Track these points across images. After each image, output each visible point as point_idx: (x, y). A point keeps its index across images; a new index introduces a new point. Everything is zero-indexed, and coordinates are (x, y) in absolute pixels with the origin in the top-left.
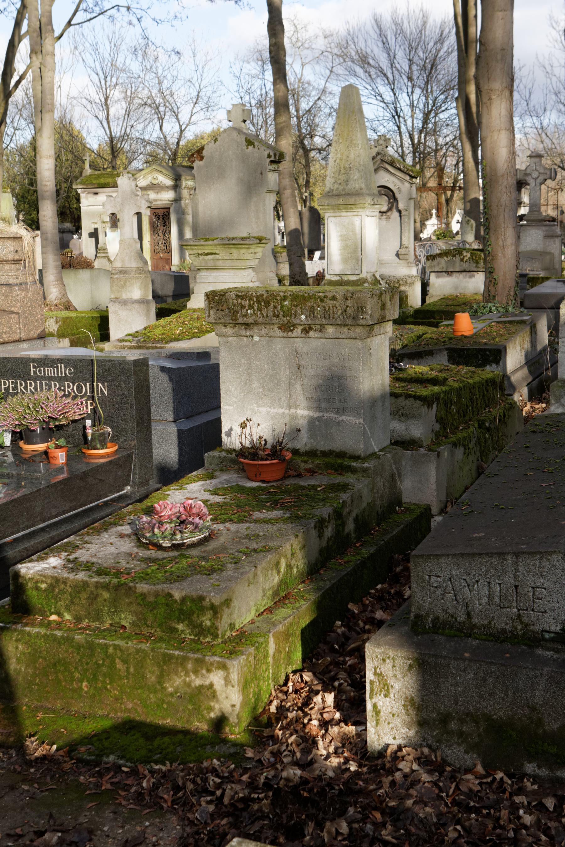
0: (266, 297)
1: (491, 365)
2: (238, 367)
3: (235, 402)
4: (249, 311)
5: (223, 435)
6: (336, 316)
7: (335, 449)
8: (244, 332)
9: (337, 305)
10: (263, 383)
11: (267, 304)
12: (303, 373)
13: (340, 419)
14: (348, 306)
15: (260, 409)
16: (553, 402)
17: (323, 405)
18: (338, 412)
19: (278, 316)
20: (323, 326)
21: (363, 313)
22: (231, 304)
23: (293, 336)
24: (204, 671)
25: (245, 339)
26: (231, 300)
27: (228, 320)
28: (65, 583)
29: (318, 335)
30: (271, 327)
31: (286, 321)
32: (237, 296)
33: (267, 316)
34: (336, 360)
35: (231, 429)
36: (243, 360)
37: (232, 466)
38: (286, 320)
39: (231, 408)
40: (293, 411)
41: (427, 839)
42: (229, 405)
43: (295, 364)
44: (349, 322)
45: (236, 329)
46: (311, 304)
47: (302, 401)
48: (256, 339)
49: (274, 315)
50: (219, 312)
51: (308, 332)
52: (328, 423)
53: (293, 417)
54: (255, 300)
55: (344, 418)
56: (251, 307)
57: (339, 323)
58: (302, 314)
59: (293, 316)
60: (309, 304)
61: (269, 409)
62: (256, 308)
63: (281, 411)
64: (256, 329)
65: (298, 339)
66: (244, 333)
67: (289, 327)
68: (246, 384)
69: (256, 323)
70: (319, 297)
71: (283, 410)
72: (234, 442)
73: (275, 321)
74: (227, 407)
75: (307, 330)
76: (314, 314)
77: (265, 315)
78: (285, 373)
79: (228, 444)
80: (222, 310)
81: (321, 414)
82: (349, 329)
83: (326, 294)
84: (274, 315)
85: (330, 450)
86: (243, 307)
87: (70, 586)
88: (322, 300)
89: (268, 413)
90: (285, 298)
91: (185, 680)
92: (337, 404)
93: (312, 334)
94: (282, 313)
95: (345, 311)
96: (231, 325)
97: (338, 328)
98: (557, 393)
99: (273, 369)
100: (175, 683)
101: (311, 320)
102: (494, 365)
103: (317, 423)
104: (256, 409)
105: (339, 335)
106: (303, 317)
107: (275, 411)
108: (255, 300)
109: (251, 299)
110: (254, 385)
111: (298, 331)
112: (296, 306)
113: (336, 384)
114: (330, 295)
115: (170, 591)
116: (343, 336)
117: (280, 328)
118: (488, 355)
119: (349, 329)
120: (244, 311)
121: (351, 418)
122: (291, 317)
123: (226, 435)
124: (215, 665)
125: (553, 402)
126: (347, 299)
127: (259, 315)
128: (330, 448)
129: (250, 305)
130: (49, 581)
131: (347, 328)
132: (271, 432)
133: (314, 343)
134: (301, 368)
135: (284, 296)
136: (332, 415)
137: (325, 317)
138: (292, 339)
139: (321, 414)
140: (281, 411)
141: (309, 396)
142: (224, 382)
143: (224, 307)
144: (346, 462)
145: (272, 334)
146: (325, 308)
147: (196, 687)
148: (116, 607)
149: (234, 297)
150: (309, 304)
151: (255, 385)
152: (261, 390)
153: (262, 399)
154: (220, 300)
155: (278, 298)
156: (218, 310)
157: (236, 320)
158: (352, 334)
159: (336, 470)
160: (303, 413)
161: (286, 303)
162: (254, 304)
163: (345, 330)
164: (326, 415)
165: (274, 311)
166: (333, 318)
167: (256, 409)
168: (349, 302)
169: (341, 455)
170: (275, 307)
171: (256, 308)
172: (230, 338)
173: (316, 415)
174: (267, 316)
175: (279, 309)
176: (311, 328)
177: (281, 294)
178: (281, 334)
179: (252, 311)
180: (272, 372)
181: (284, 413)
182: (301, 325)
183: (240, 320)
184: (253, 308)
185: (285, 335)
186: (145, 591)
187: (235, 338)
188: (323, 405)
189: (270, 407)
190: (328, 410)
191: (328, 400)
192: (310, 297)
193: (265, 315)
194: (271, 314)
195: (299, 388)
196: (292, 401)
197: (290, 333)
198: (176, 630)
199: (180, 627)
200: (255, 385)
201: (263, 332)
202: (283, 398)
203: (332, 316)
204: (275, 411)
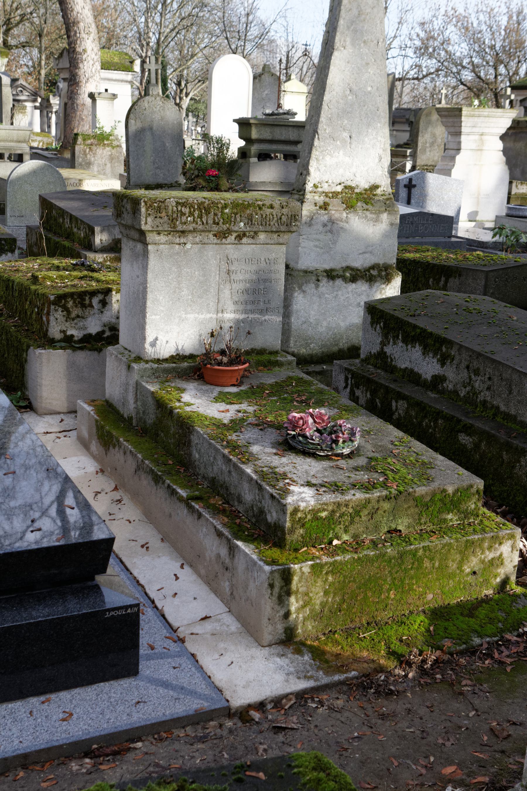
0: (208, 205)
1: (7, 254)
2: (168, 275)
3: (163, 311)
4: (189, 219)
5: (147, 346)
6: (272, 223)
7: (257, 347)
8: (178, 239)
9: (274, 213)
10: (193, 290)
11: (208, 212)
12: (232, 278)
13: (263, 319)
14: (283, 214)
15: (188, 316)
16: (297, 289)
17: (249, 307)
18: (262, 312)
19: (218, 224)
20: (256, 233)
21: (296, 220)
22: (170, 211)
23: (226, 242)
24: (497, 546)
25: (177, 246)
26: (170, 207)
27: (166, 227)
28: (347, 506)
29: (250, 241)
30: (207, 234)
31: (225, 228)
32: (178, 203)
33: (207, 223)
34: (263, 265)
35: (156, 339)
36: (174, 268)
37: (165, 376)
38: (225, 227)
39: (158, 317)
40: (220, 315)
41: (503, 634)
42: (156, 315)
43: (225, 270)
44: (283, 228)
45: (170, 236)
46: (251, 212)
47: (230, 306)
48: (188, 246)
49: (214, 223)
50: (158, 220)
51: (241, 239)
52: (252, 323)
53: (220, 321)
54: (196, 207)
55: (267, 317)
56: (191, 214)
57: (274, 230)
58: (241, 221)
59: (233, 224)
60: (248, 212)
61: (196, 315)
62: (196, 215)
63: (209, 316)
64: (190, 237)
65: (230, 246)
66: (177, 240)
67: (225, 234)
68: (175, 292)
69: (195, 230)
70: (258, 205)
71: (211, 315)
72: (158, 351)
73: (215, 228)
74: (154, 317)
75: (240, 237)
76: (251, 221)
77: (205, 222)
78: (215, 278)
79: (152, 355)
80: (160, 217)
81: (247, 316)
82: (279, 236)
83: (265, 202)
84: (214, 223)
85: (252, 349)
86: (185, 214)
87: (352, 507)
88: (260, 208)
89: (196, 319)
90: (225, 206)
91: (481, 558)
92: (262, 305)
93: (244, 240)
94: (222, 220)
95: (281, 218)
96: (166, 233)
97: (270, 234)
98: (300, 282)
99: (204, 275)
100: (474, 562)
101: (250, 227)
102: (9, 254)
103: (242, 324)
104: (184, 316)
105: (269, 241)
106: (242, 224)
107: (202, 317)
108: (196, 207)
109: (191, 206)
110: (183, 293)
111: (232, 238)
112: (236, 214)
113: (262, 287)
114: (268, 203)
115: (445, 487)
116: (272, 242)
117: (215, 235)
118: (4, 245)
119: (279, 236)
120: (184, 219)
121: (273, 317)
122: (230, 224)
123: (151, 345)
124: (506, 537)
125: (297, 289)
126: (283, 208)
127: (199, 223)
128: (252, 346)
129: (190, 212)
130: (330, 508)
131: (277, 234)
132: (198, 337)
133: (247, 248)
134: (231, 274)
135: (225, 204)
136: (257, 316)
137: (262, 225)
138: (224, 246)
139: (247, 316)
140: (209, 316)
141: (237, 300)
142: (152, 292)
143: (163, 214)
144: (272, 358)
145: (206, 241)
146: (262, 215)
147: (489, 561)
148: (394, 516)
149: (174, 204)
150: (248, 212)
151: (185, 292)
152: (190, 297)
153: (190, 306)
154: (159, 207)
155: (220, 206)
156: (156, 217)
157: (174, 227)
158: (281, 240)
159: (265, 366)
160: (230, 316)
161: (227, 211)
162: (194, 211)
163: (275, 236)
164: (251, 316)
165: (214, 219)
166: (269, 225)
167: (184, 316)
168: (284, 210)
169: (261, 352)
170: (215, 214)
171: (196, 215)
172: (162, 246)
173: (242, 317)
174: (207, 223)
175: (219, 217)
176: (244, 235)
177: (222, 201)
178: (216, 241)
179: (192, 218)
180: (201, 278)
181: (211, 318)
182: (236, 232)
183: (180, 228)
184: (193, 215)
185: (219, 241)
186: (423, 492)
187: (167, 246)
188: (249, 307)
189: (198, 313)
190: (252, 312)
191: (253, 302)
192: (249, 205)
193: (205, 222)
194: (210, 221)
195: (226, 293)
196: (220, 305)
197: (224, 240)
198: (445, 520)
199: (450, 516)
200: (185, 292)
201: (197, 240)
202: (211, 304)
203: (268, 223)
204: (202, 317)
